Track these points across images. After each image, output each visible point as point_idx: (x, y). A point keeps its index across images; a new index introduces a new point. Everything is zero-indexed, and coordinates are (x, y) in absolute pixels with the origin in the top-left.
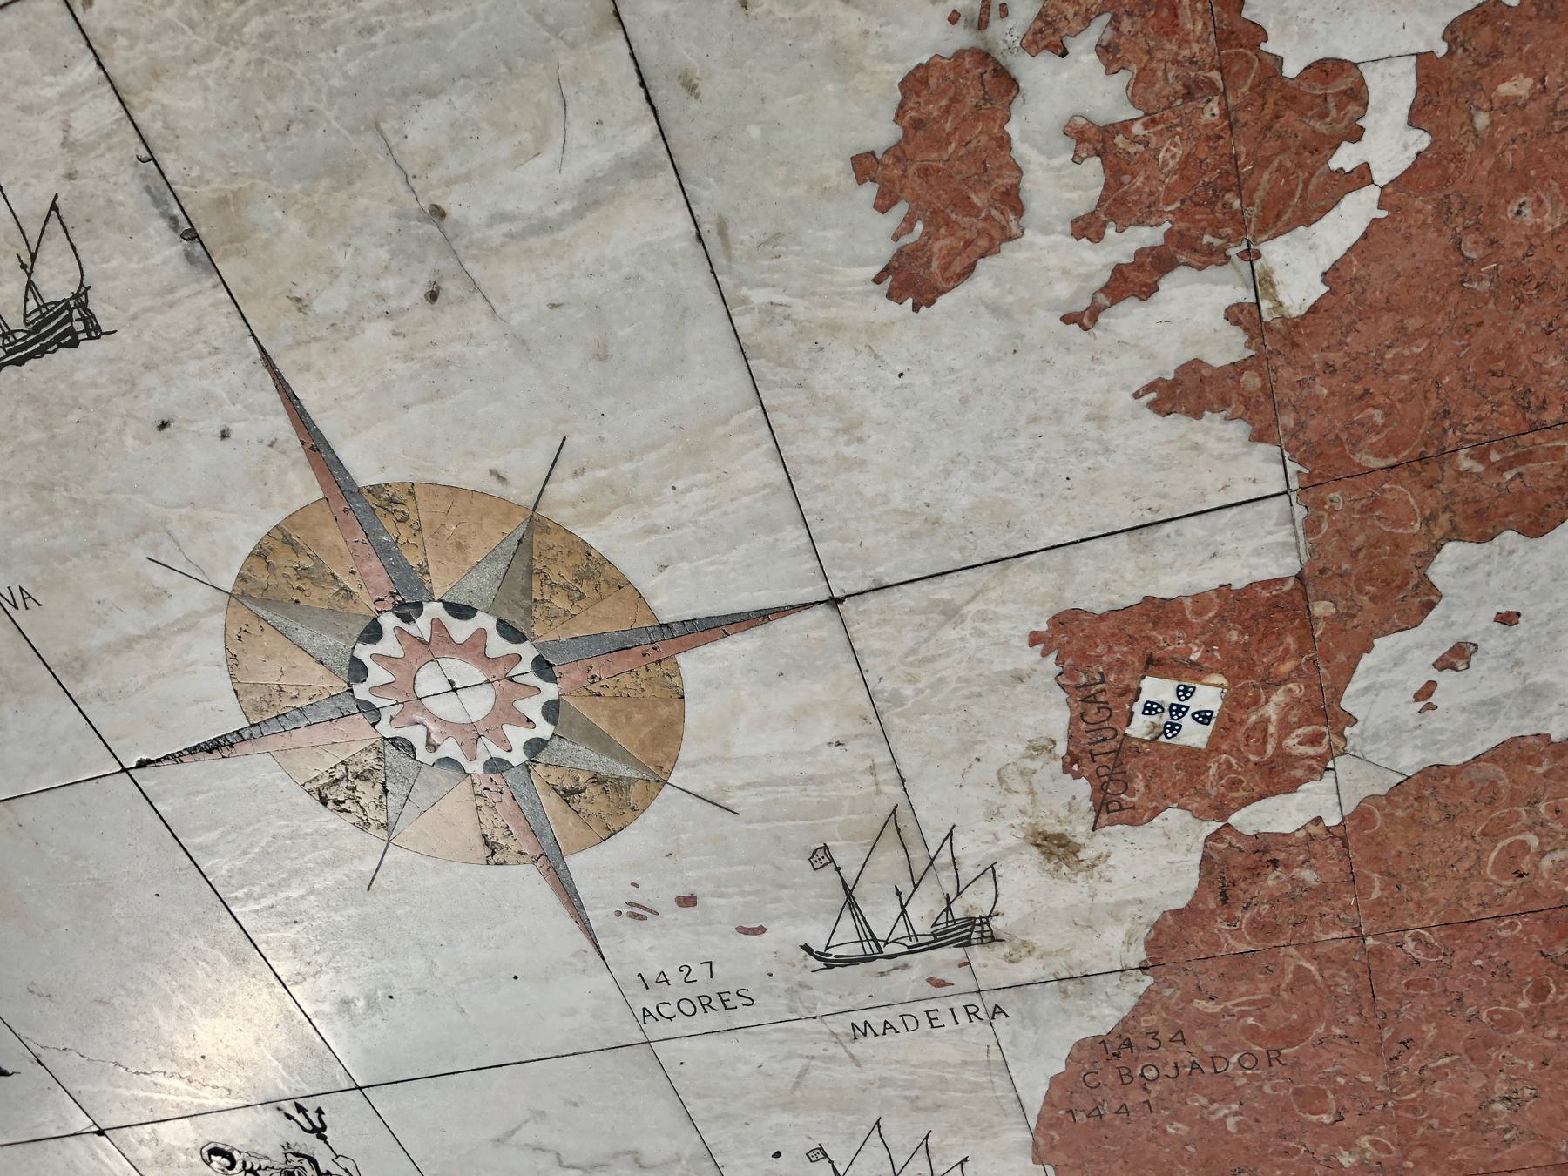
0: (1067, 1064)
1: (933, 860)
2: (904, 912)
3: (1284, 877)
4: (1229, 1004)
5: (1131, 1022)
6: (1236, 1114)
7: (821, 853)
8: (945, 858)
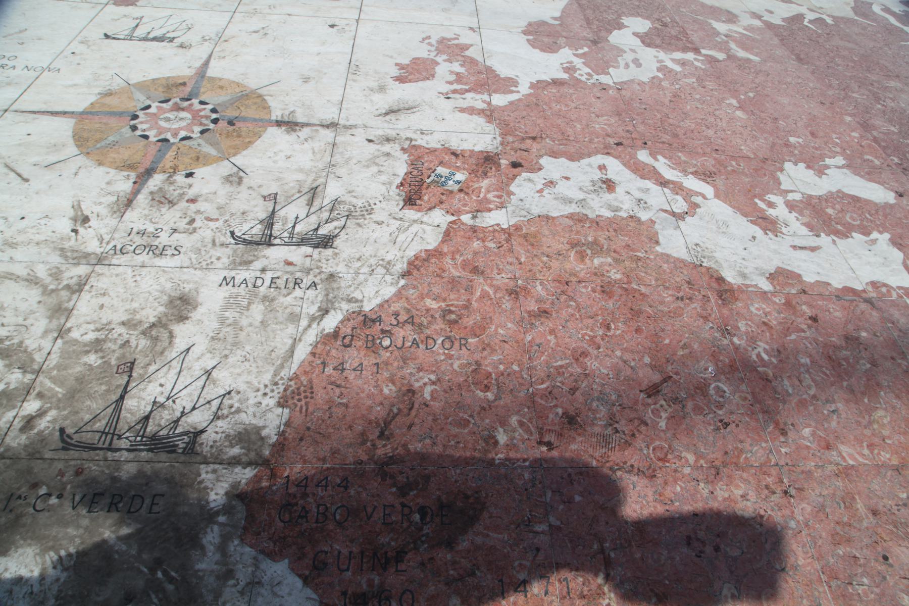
6: (434, 383)
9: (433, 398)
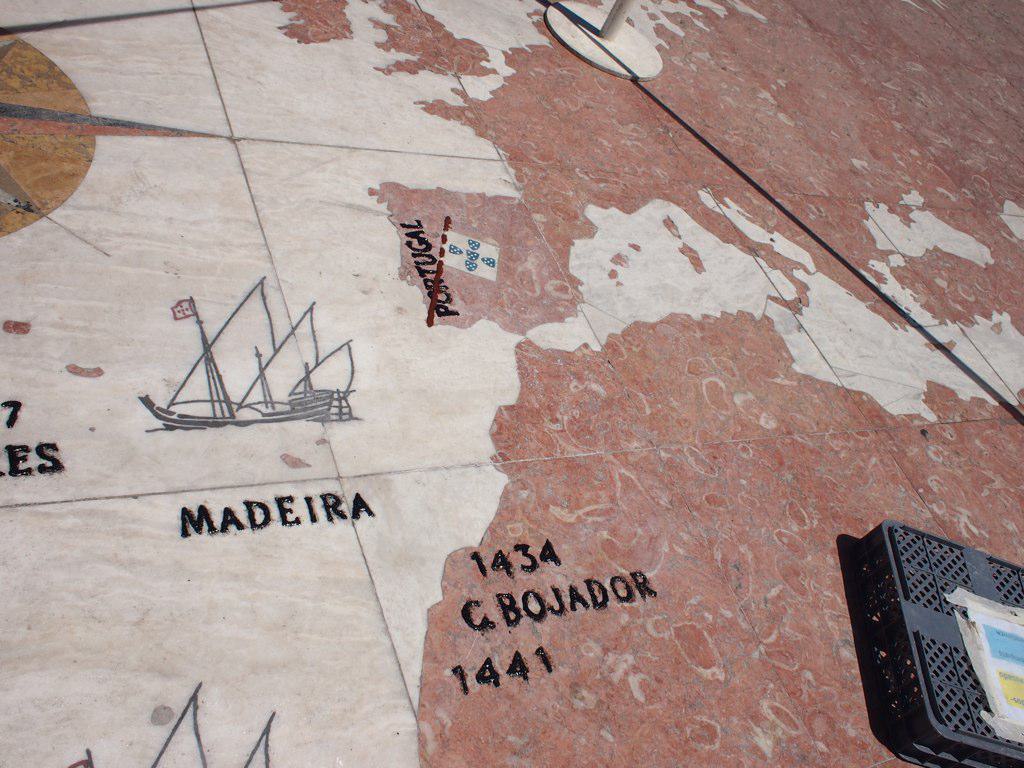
0: (444, 590)
1: (294, 329)
2: (262, 375)
3: (581, 387)
4: (580, 512)
5: (498, 530)
6: (635, 669)
7: (186, 305)
8: (305, 328)
9: (649, 699)
